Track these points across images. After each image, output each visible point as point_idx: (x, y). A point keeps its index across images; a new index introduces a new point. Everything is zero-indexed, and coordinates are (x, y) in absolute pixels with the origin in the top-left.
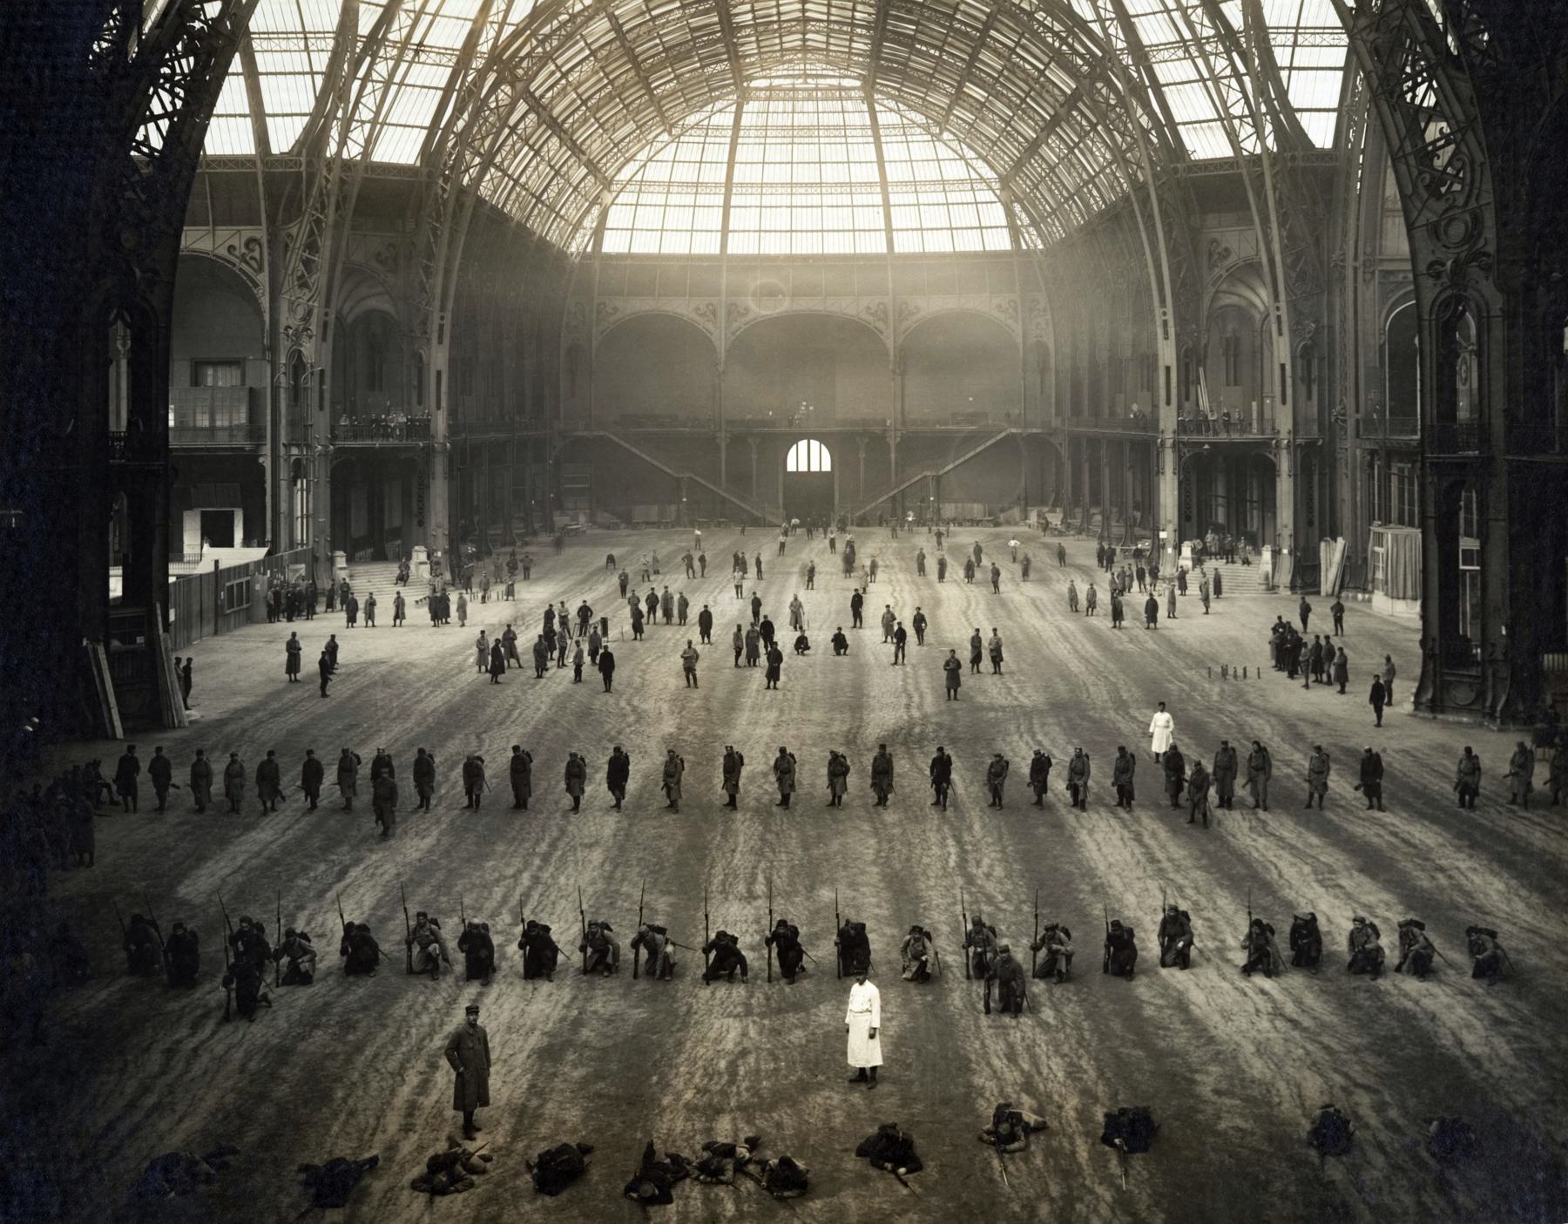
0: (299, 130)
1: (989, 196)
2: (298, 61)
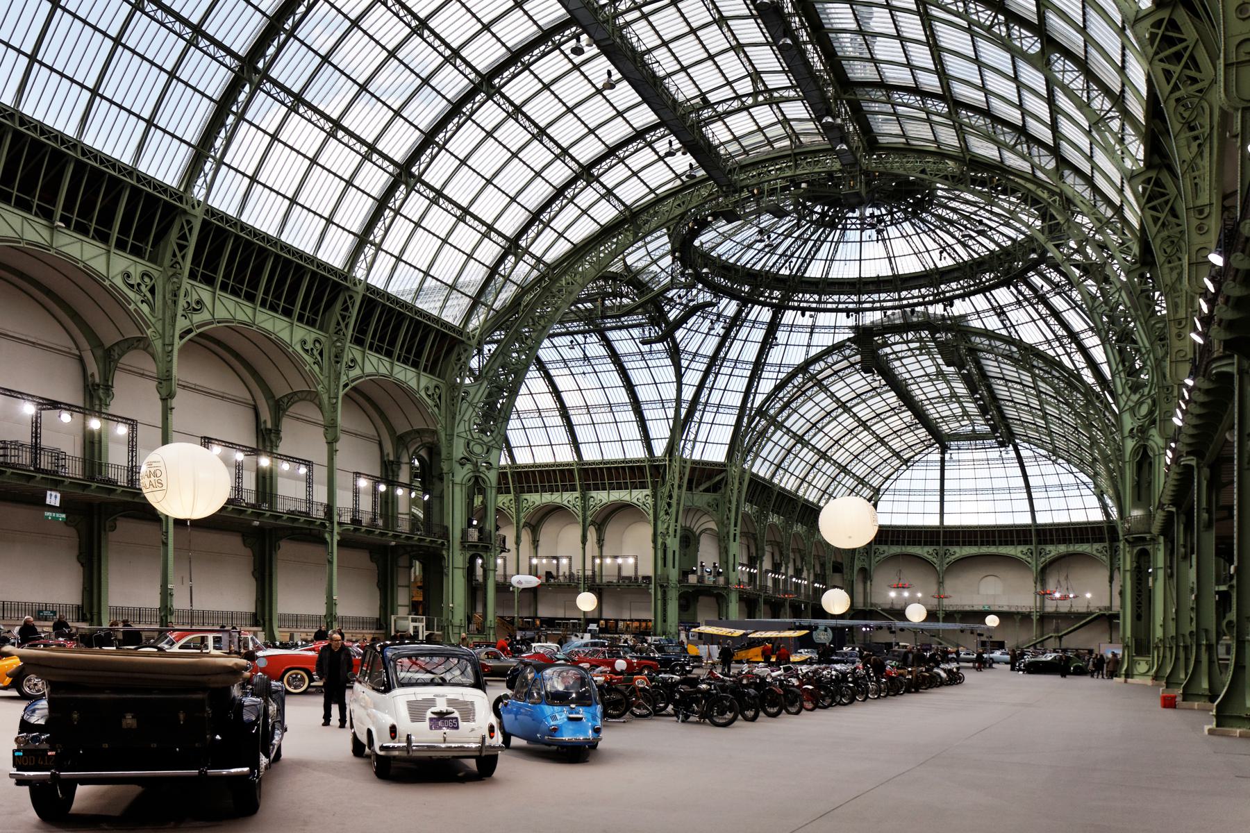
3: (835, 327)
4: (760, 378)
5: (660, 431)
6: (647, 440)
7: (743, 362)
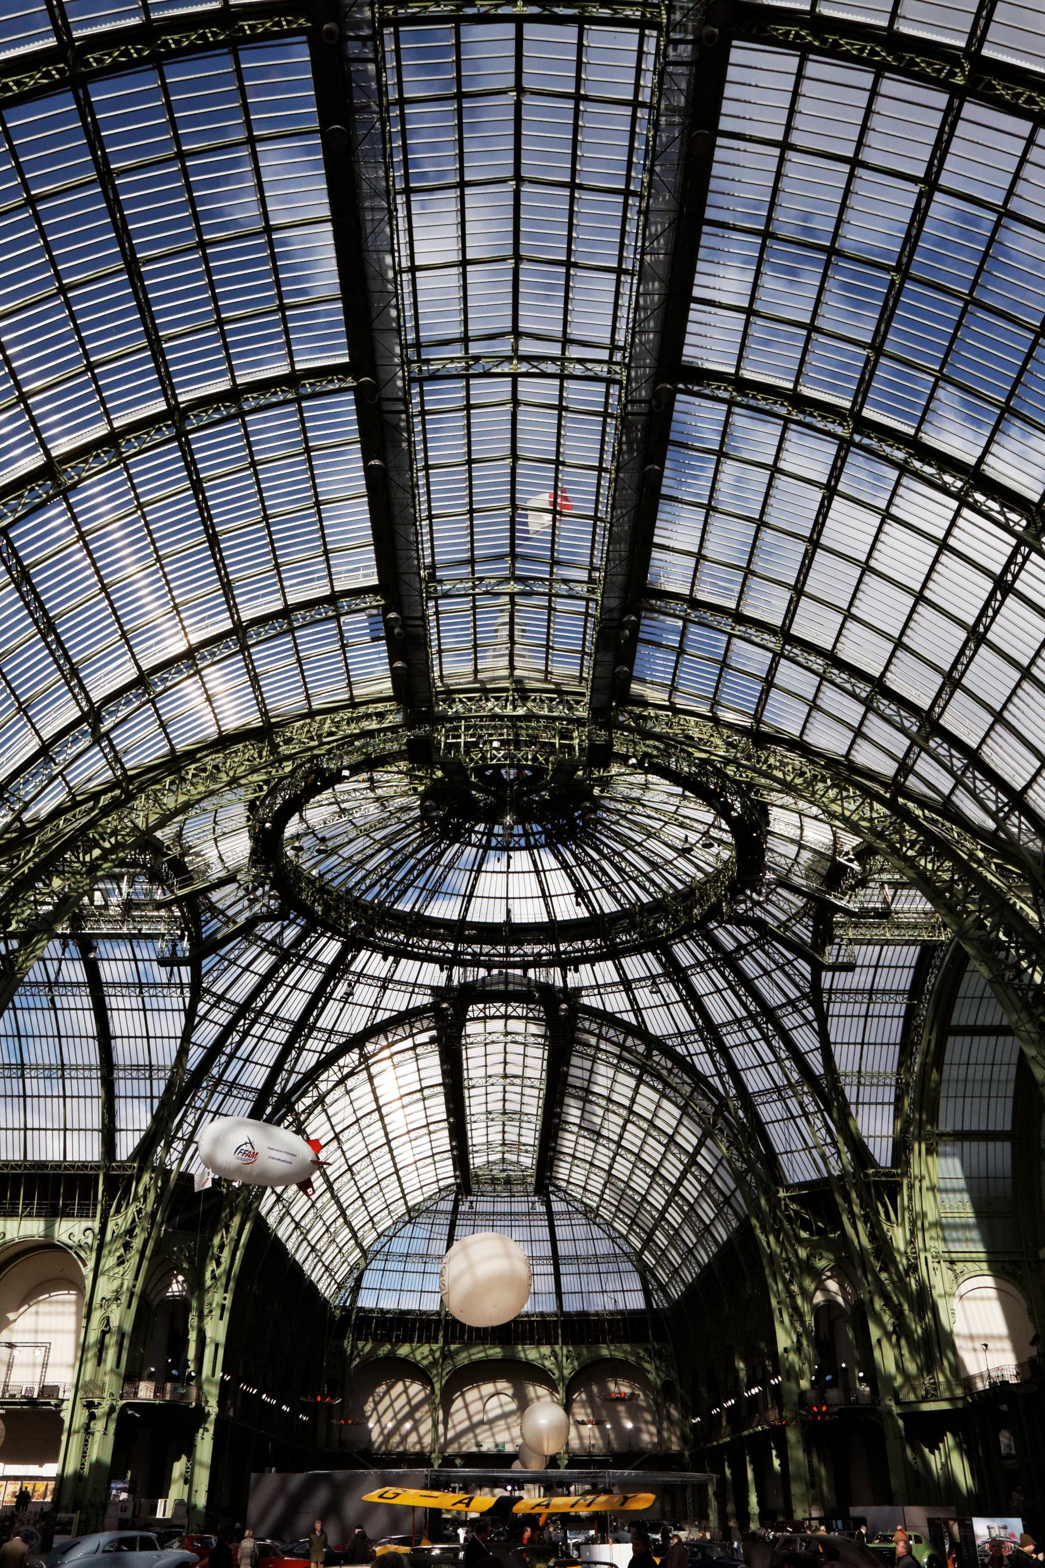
0: (137, 1141)
1: (629, 1266)
2: (142, 1087)
3: (415, 985)
4: (302, 1049)
5: (135, 1119)
6: (109, 1132)
7: (283, 1020)
